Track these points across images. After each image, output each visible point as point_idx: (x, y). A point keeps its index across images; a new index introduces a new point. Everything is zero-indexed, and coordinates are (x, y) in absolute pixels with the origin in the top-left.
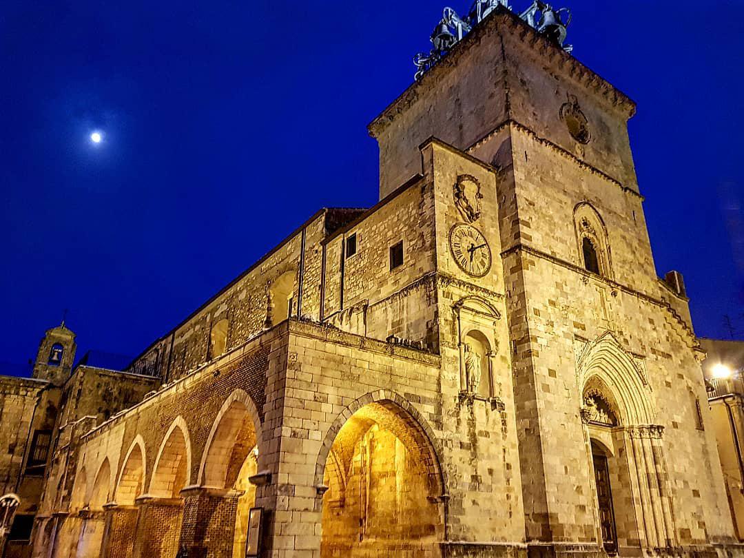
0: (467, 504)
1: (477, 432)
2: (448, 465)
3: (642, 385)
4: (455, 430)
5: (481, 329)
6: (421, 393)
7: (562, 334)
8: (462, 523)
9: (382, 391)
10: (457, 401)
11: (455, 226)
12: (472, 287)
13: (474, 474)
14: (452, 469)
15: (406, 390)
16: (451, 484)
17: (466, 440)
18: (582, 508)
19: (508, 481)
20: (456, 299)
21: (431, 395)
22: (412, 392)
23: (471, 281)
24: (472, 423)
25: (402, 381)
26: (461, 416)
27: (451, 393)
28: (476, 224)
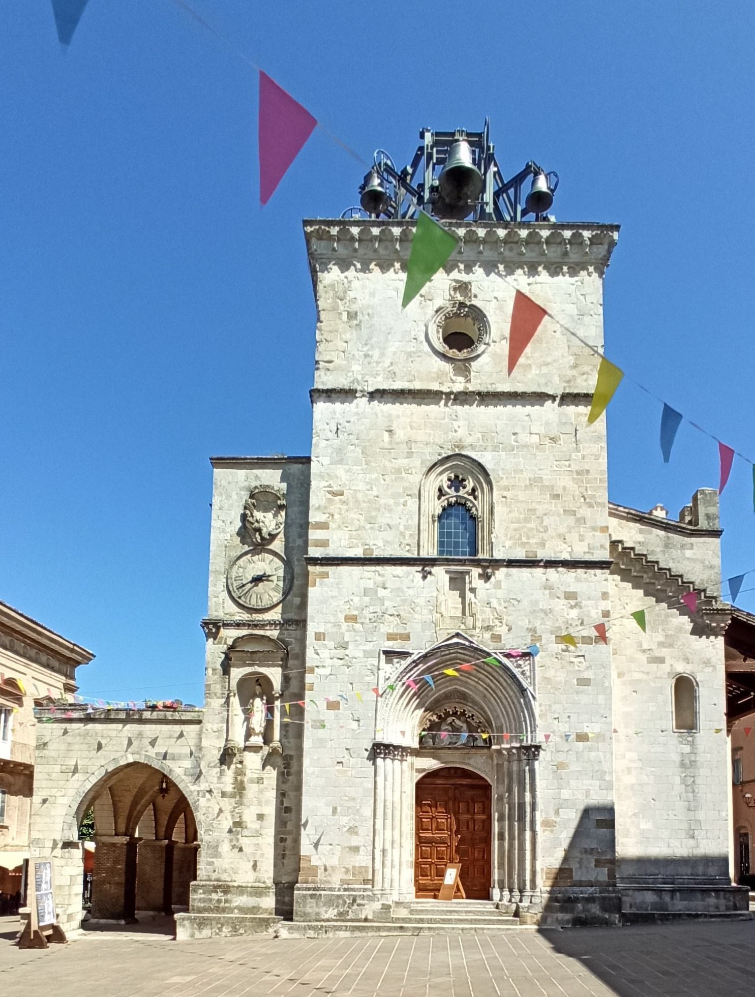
0: (225, 847)
1: (246, 779)
2: (204, 814)
4: (215, 780)
7: (361, 654)
8: (215, 865)
13: (238, 820)
14: (208, 817)
16: (206, 831)
17: (229, 788)
18: (356, 849)
24: (240, 773)
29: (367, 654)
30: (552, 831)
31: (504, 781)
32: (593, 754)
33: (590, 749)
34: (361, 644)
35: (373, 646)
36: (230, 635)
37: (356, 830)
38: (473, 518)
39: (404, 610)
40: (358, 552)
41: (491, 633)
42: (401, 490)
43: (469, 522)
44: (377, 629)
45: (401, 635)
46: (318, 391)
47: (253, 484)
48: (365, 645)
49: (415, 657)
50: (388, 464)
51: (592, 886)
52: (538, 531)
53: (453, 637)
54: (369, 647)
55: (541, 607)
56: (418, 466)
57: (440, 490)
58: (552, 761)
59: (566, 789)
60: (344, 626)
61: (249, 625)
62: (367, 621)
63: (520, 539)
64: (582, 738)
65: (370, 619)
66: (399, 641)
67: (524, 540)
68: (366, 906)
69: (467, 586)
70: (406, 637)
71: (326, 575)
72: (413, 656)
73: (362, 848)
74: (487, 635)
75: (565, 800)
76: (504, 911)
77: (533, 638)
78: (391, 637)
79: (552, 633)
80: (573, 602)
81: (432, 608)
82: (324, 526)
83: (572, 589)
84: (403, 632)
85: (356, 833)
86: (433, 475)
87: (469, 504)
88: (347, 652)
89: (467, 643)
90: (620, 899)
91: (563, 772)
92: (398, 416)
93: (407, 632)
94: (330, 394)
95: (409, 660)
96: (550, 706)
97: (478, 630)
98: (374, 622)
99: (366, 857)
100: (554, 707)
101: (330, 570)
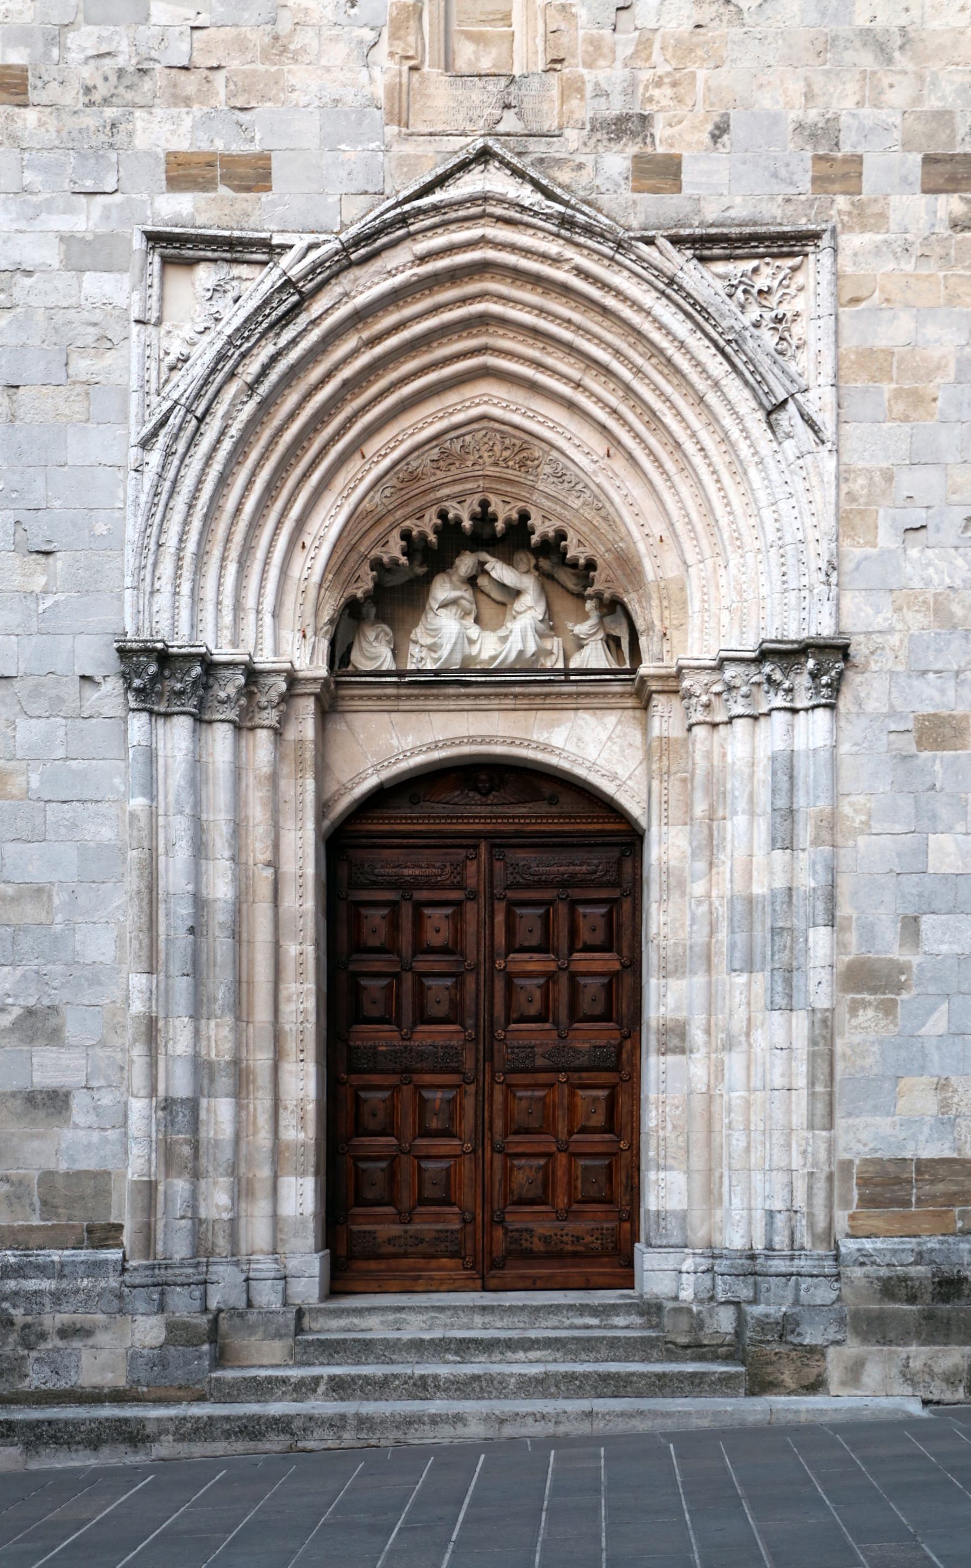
3: (755, 421)
7: (51, 255)
30: (888, 1009)
31: (689, 807)
34: (49, 207)
35: (106, 214)
37: (53, 1022)
39: (241, 45)
41: (633, 149)
44: (120, 138)
45: (229, 161)
48: (69, 210)
53: (463, 166)
55: (861, 21)
58: (893, 713)
59: (949, 830)
62: (71, 97)
65: (88, 90)
66: (223, 190)
68: (101, 1338)
72: (285, 261)
73: (79, 1101)
75: (945, 876)
76: (683, 1340)
77: (824, 167)
79: (907, 145)
81: (370, 36)
84: (238, 147)
85: (55, 1037)
89: (528, 196)
93: (256, 148)
96: (889, 477)
98: (106, 101)
99: (95, 1136)
100: (907, 481)
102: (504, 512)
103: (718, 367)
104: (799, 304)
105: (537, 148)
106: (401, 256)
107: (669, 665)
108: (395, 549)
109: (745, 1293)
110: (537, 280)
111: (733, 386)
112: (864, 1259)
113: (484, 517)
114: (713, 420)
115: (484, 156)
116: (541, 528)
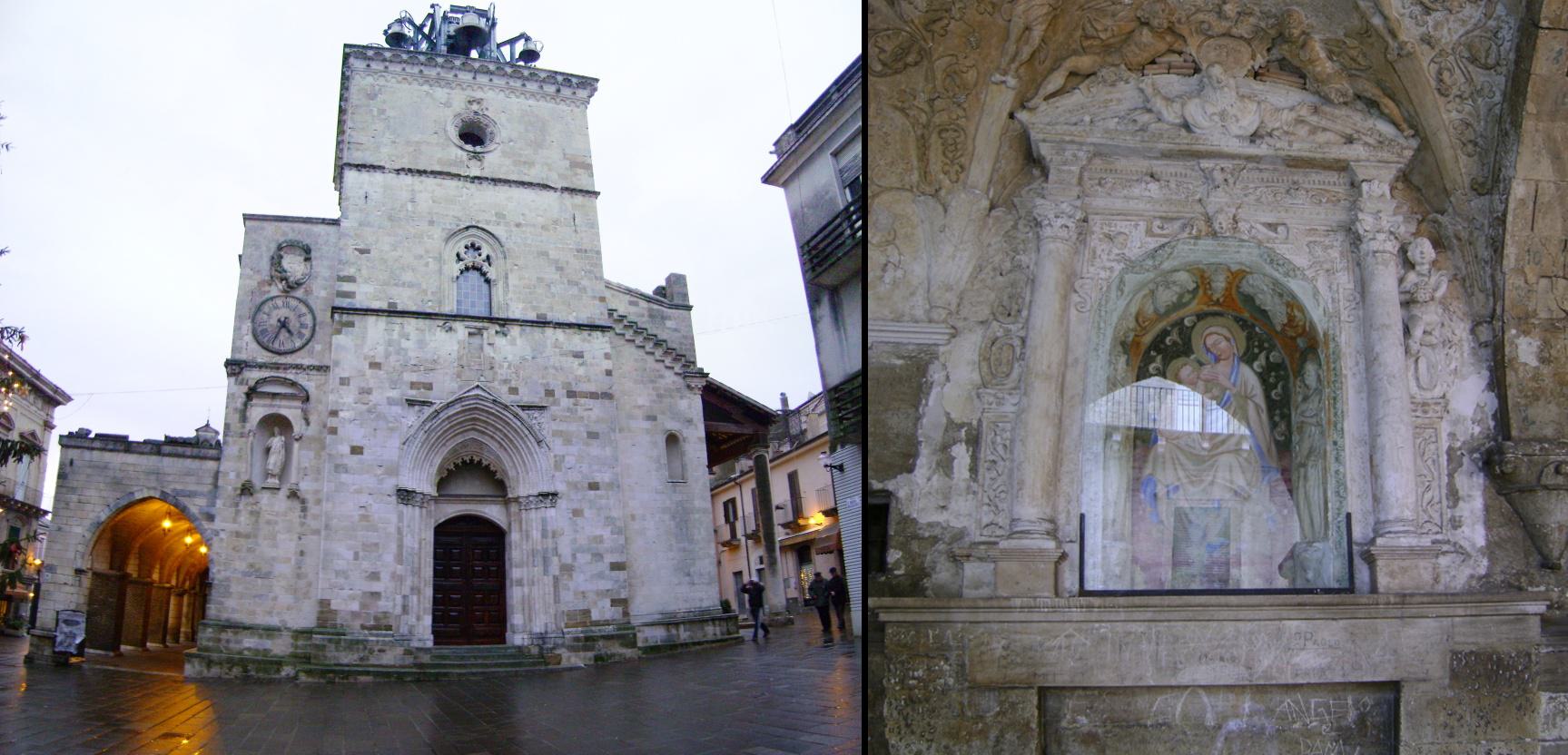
3: (535, 444)
5: (284, 412)
6: (192, 488)
9: (145, 490)
10: (239, 492)
11: (263, 303)
12: (277, 367)
15: (172, 487)
19: (300, 568)
20: (252, 383)
21: (207, 488)
22: (179, 487)
23: (282, 360)
24: (256, 514)
25: (170, 479)
26: (241, 507)
27: (230, 482)
28: (299, 293)
29: (391, 402)
32: (603, 501)
33: (601, 497)
36: (253, 375)
38: (488, 281)
40: (384, 306)
42: (423, 253)
43: (485, 286)
46: (349, 165)
47: (282, 239)
49: (435, 407)
50: (411, 230)
51: (609, 625)
52: (547, 297)
54: (394, 394)
55: (551, 363)
56: (438, 234)
57: (458, 255)
60: (369, 372)
61: (272, 368)
63: (531, 302)
64: (594, 486)
67: (535, 304)
69: (485, 342)
70: (429, 387)
71: (351, 324)
74: (505, 389)
78: (413, 385)
80: (581, 361)
82: (351, 279)
83: (579, 349)
84: (426, 381)
86: (451, 243)
87: (485, 269)
88: (371, 397)
89: (487, 395)
90: (635, 635)
91: (579, 520)
92: (421, 192)
94: (360, 167)
95: (432, 410)
97: (496, 383)
101: (356, 319)
102: (476, 459)
103: (527, 432)
104: (543, 420)
105: (489, 384)
106: (457, 406)
107: (515, 495)
108: (452, 467)
109: (541, 642)
110: (487, 412)
111: (530, 436)
112: (569, 633)
113: (472, 460)
114: (525, 443)
115: (478, 386)
116: (485, 463)
